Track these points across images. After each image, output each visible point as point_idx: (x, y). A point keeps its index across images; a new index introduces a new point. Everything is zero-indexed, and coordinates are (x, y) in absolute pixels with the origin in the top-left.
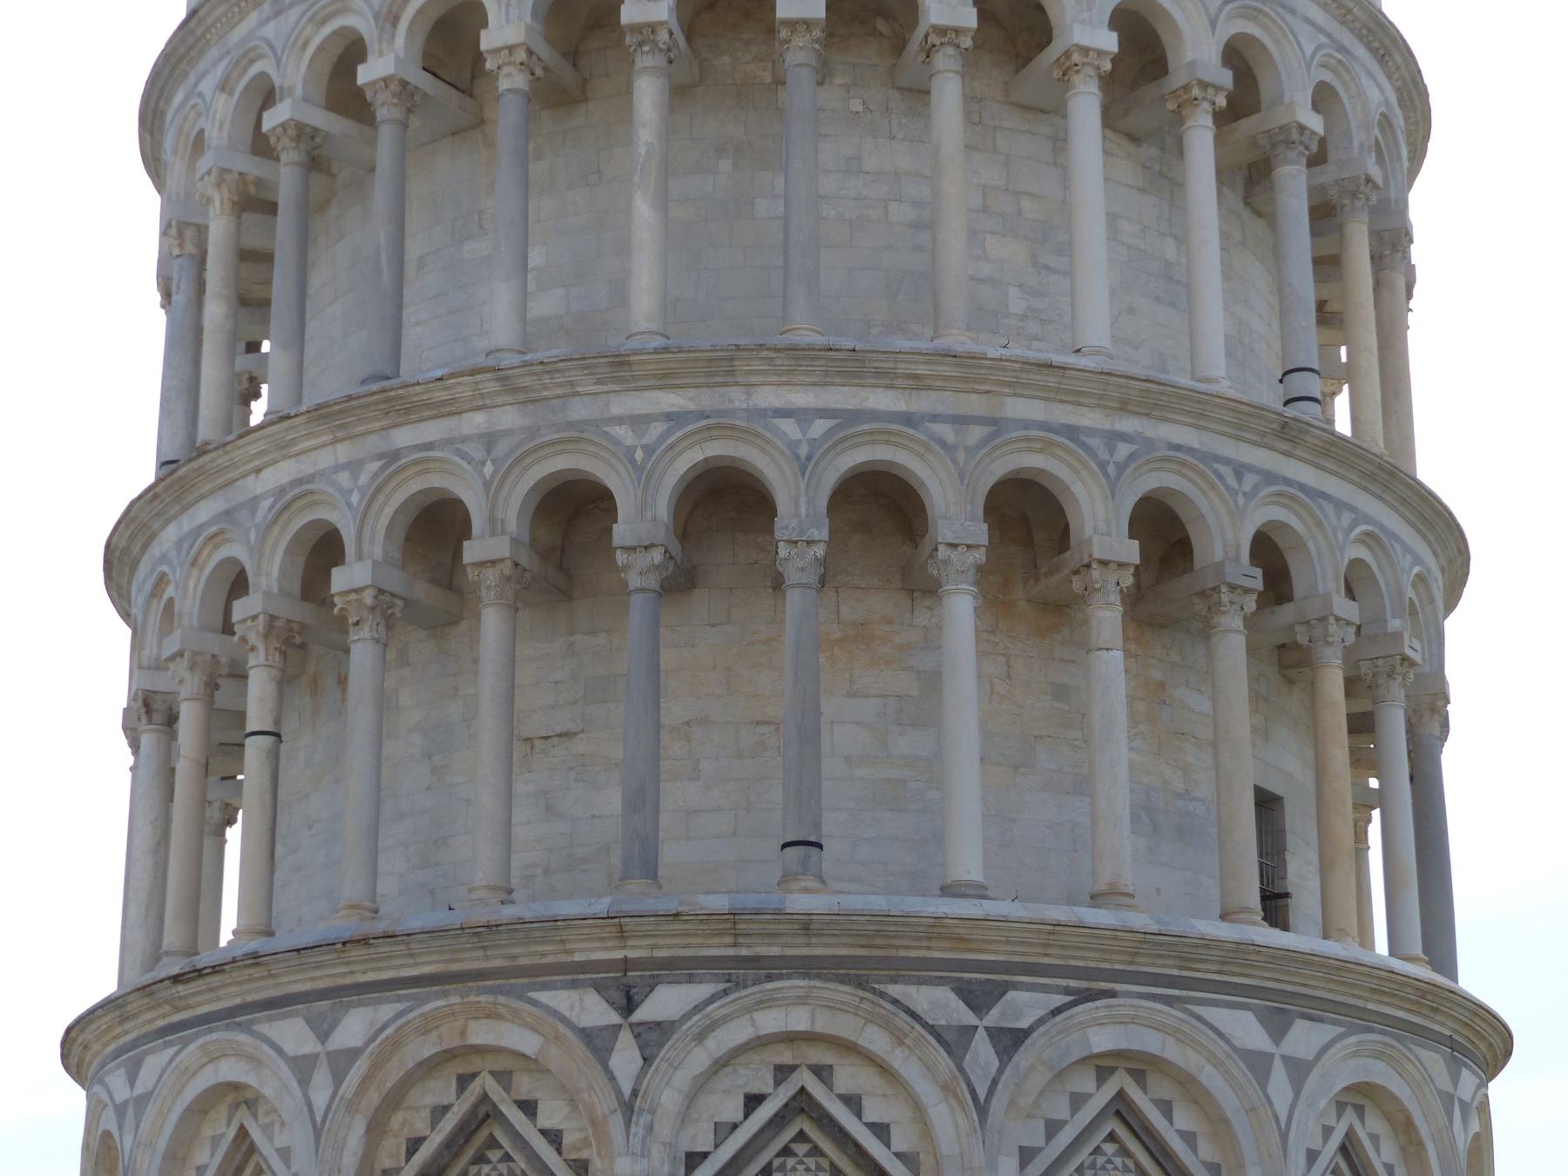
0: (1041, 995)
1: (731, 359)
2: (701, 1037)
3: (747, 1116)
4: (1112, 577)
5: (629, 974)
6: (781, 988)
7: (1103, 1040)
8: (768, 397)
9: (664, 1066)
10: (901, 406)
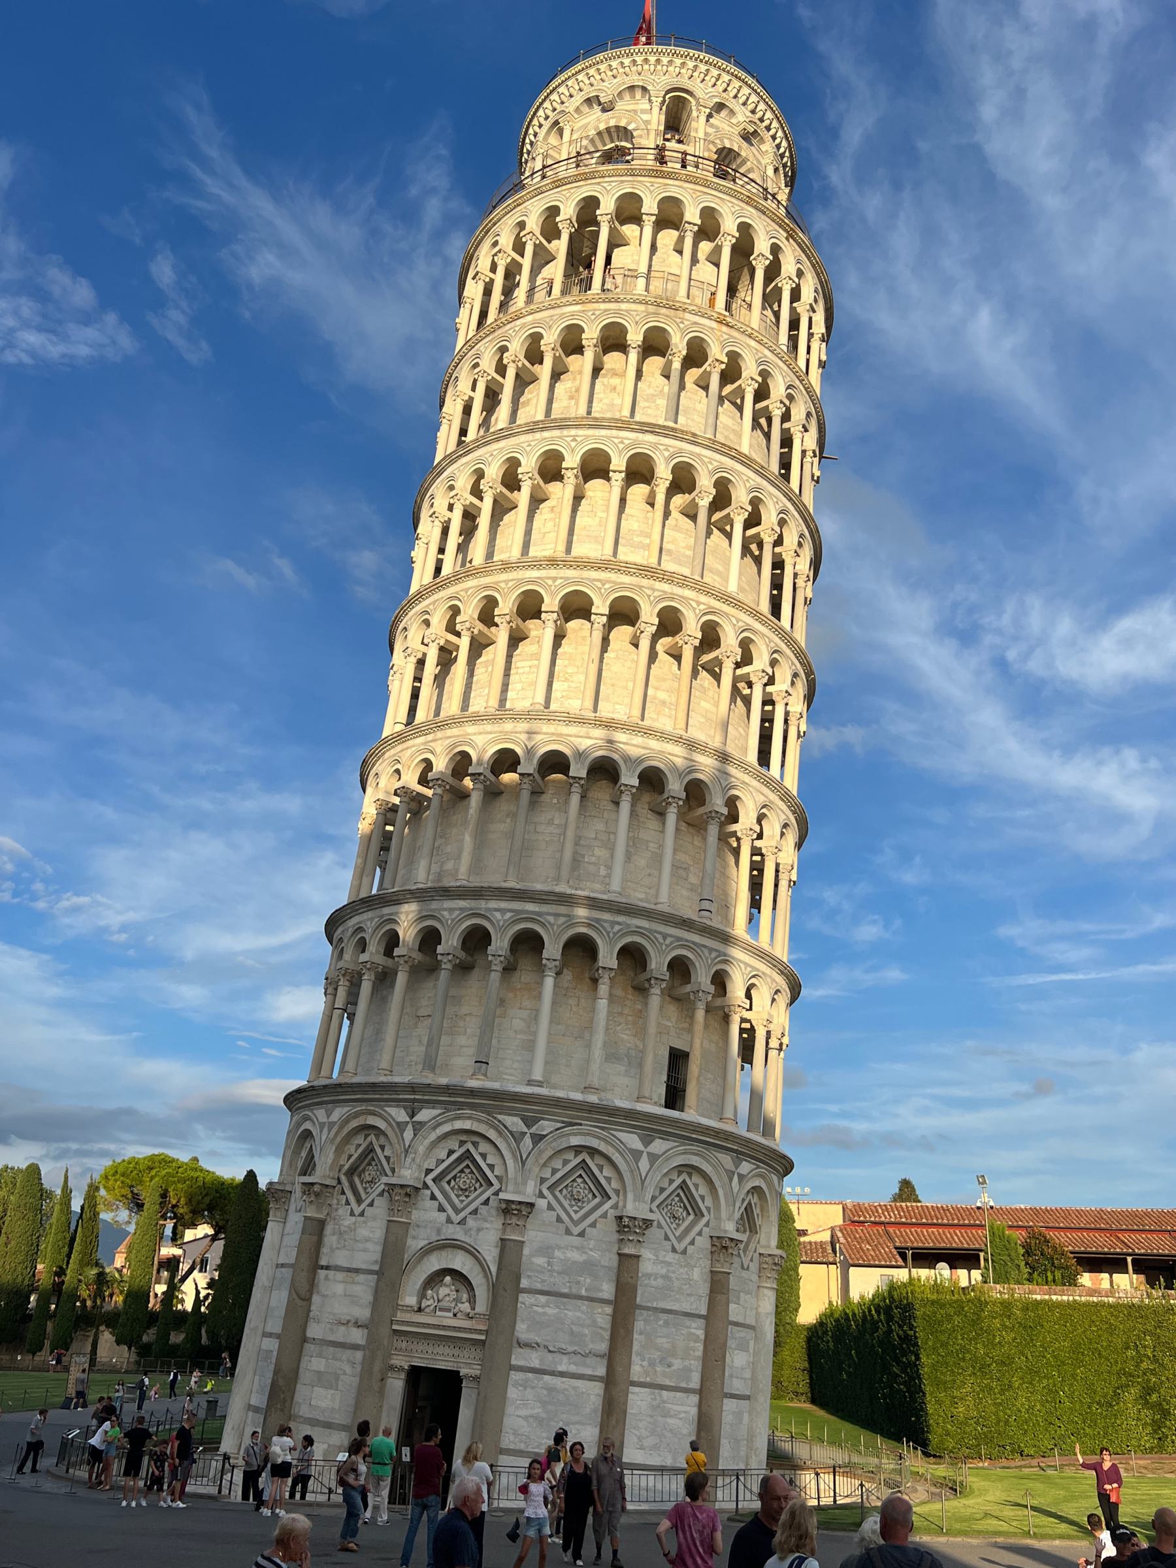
2: (434, 1128)
7: (575, 1141)
10: (537, 909)
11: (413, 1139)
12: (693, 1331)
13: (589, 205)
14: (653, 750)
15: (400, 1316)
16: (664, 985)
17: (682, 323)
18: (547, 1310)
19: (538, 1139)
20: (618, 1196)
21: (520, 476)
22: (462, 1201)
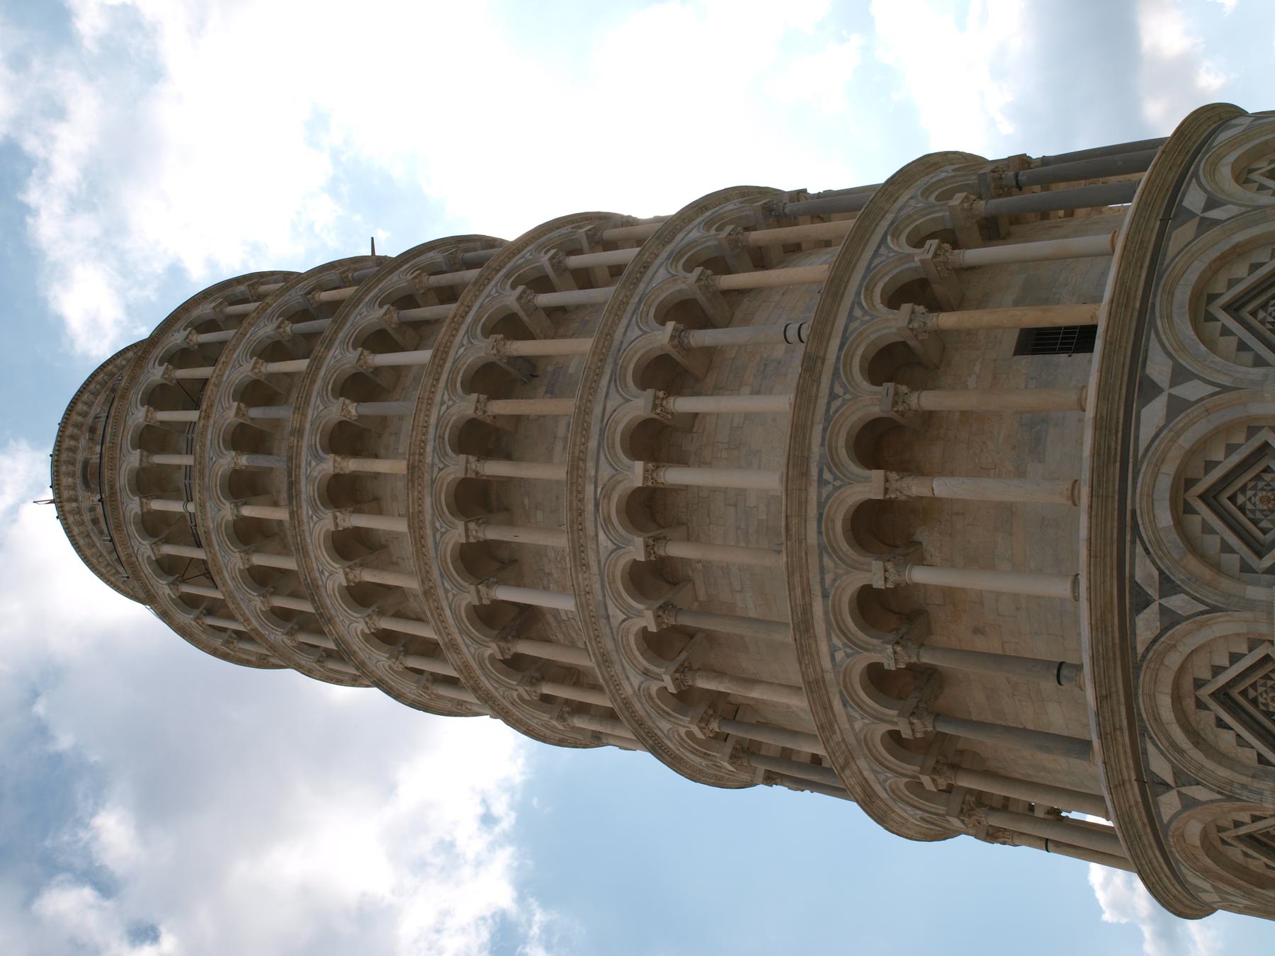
0: (1137, 560)
1: (809, 683)
2: (1181, 751)
3: (1232, 729)
4: (894, 485)
5: (1146, 780)
6: (1145, 709)
7: (1165, 518)
8: (827, 663)
9: (1200, 774)
10: (820, 599)
11: (1204, 786)
14: (599, 445)
16: (904, 389)
17: (212, 459)
19: (1168, 586)
20: (1259, 428)
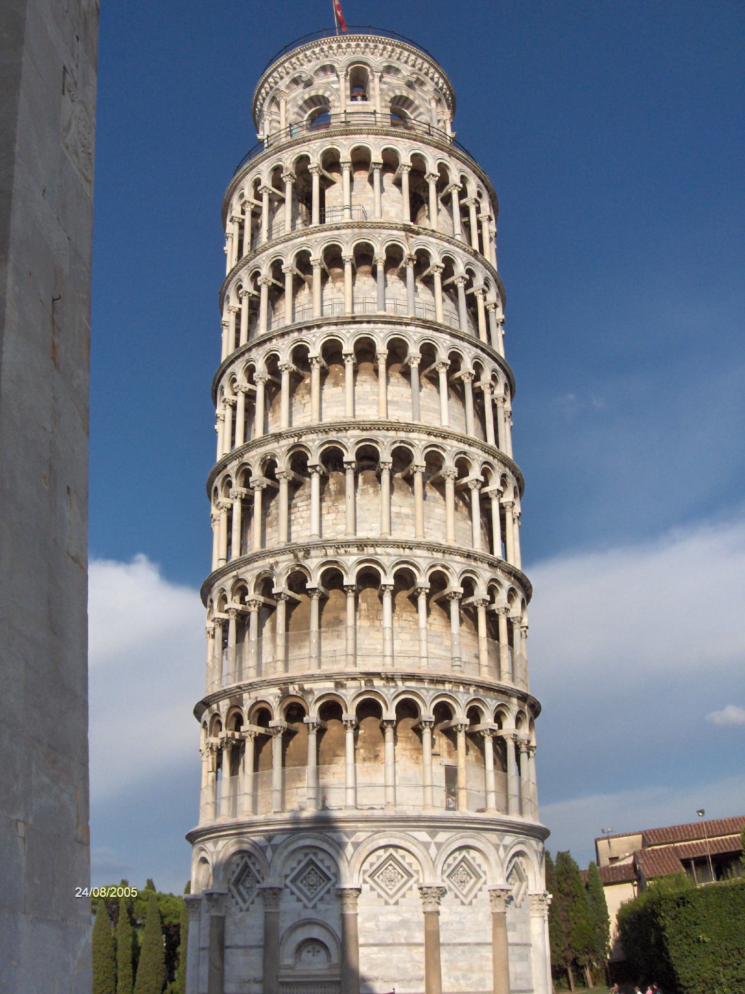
2: (286, 847)
7: (382, 842)
12: (483, 954)
13: (303, 160)
14: (400, 556)
15: (283, 972)
17: (380, 236)
18: (379, 955)
21: (280, 368)
22: (312, 893)
